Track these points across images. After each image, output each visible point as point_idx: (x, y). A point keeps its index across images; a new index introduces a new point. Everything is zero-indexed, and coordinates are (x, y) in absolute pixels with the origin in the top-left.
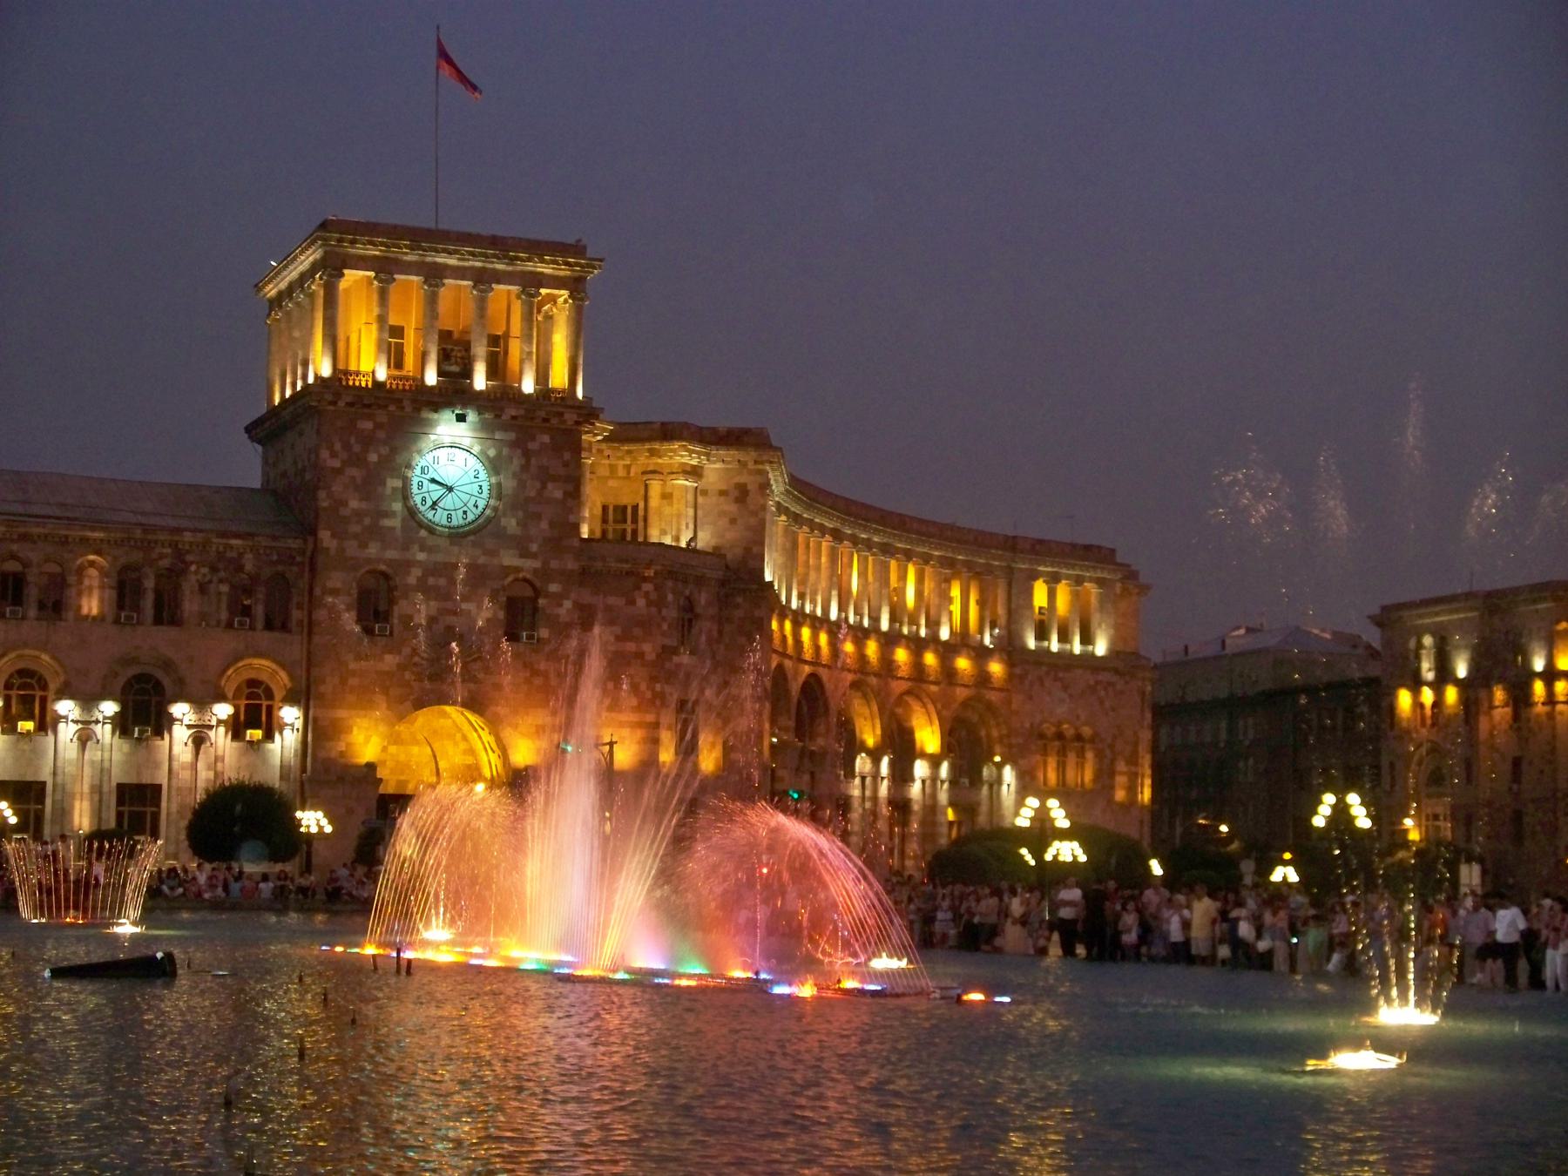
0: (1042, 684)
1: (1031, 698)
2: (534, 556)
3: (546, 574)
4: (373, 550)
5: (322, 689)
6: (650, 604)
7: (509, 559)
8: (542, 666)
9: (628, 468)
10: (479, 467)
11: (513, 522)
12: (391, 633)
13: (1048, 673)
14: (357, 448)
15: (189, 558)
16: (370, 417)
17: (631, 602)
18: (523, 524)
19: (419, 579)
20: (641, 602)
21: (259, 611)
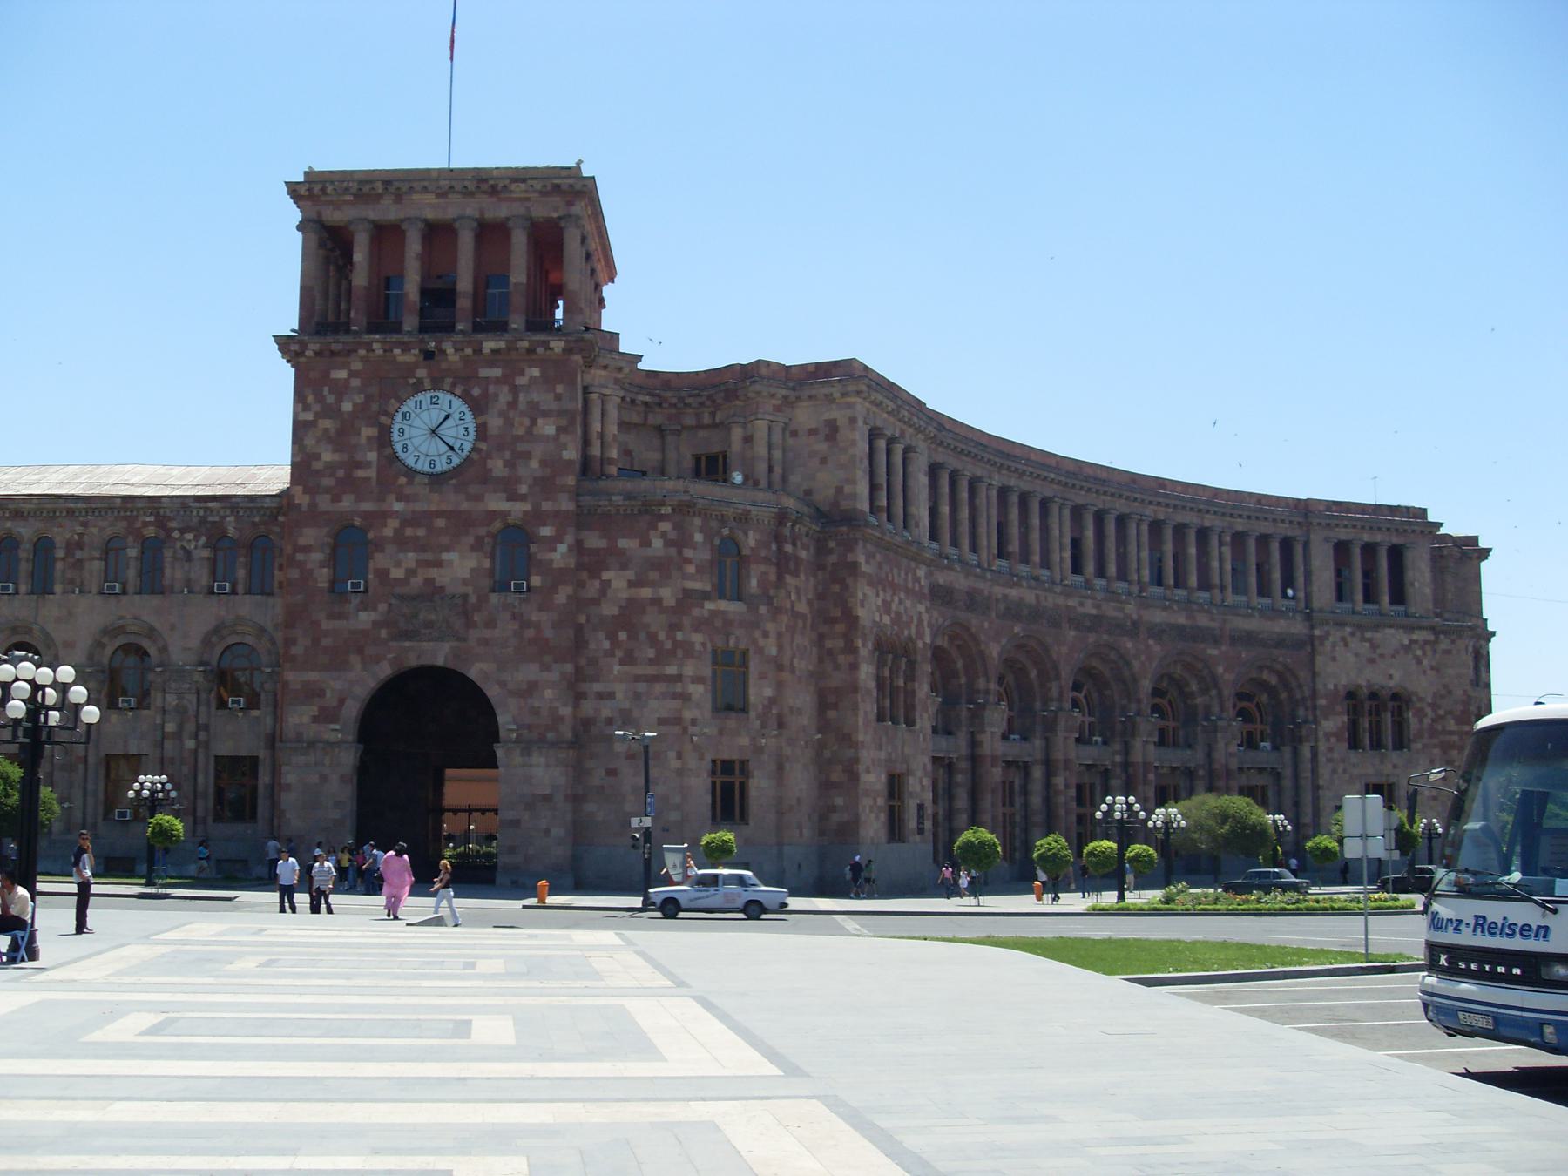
0: (1346, 645)
1: (1334, 659)
2: (523, 498)
3: (538, 517)
4: (347, 503)
5: (294, 651)
6: (669, 544)
7: (496, 503)
8: (534, 618)
9: (713, 414)
10: (465, 408)
11: (500, 463)
12: (366, 591)
13: (1352, 634)
14: (330, 399)
15: (173, 524)
16: (345, 366)
17: (646, 543)
18: (510, 464)
19: (396, 531)
20: (657, 543)
21: (241, 573)
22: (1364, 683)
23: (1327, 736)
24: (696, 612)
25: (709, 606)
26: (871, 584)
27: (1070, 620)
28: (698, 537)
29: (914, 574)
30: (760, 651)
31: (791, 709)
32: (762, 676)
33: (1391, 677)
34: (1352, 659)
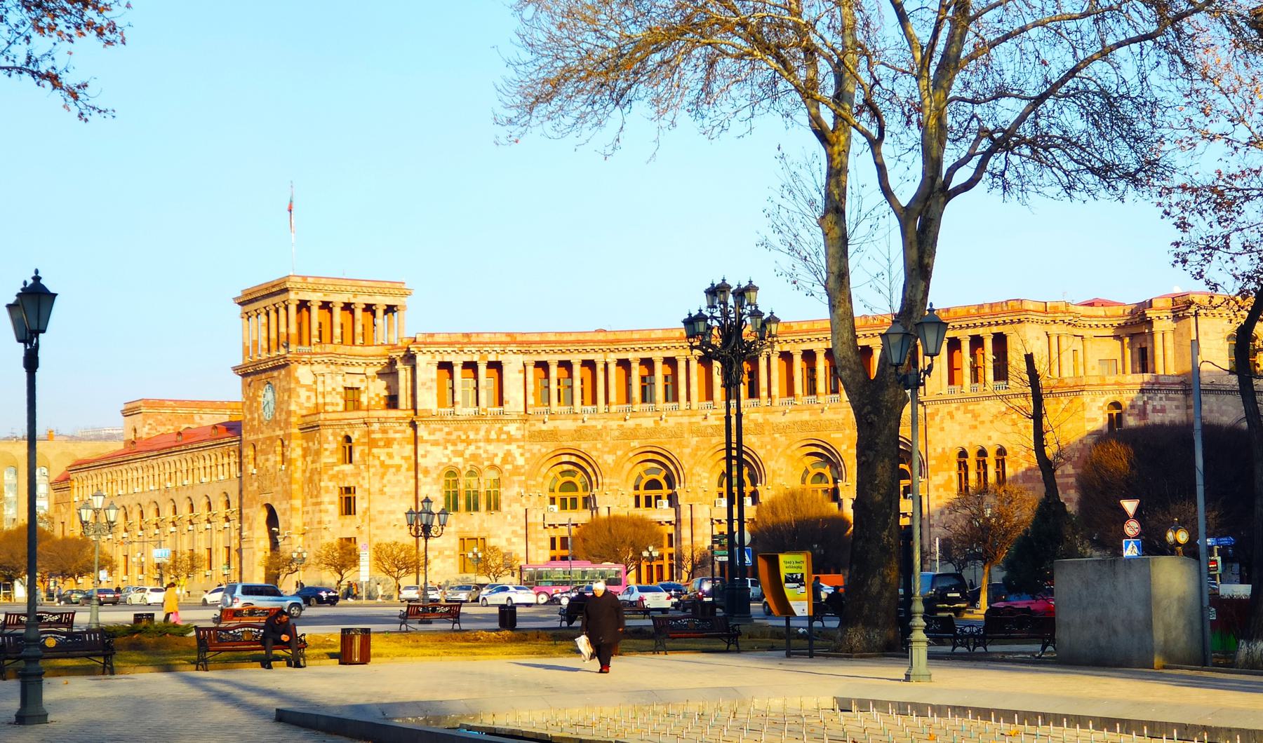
0: (952, 417)
1: (942, 429)
13: (958, 409)
22: (966, 446)
23: (937, 488)
24: (330, 472)
25: (336, 469)
26: (435, 443)
27: (692, 432)
28: (331, 438)
29: (501, 429)
30: (361, 486)
31: (382, 512)
32: (362, 498)
33: (990, 438)
34: (958, 428)
